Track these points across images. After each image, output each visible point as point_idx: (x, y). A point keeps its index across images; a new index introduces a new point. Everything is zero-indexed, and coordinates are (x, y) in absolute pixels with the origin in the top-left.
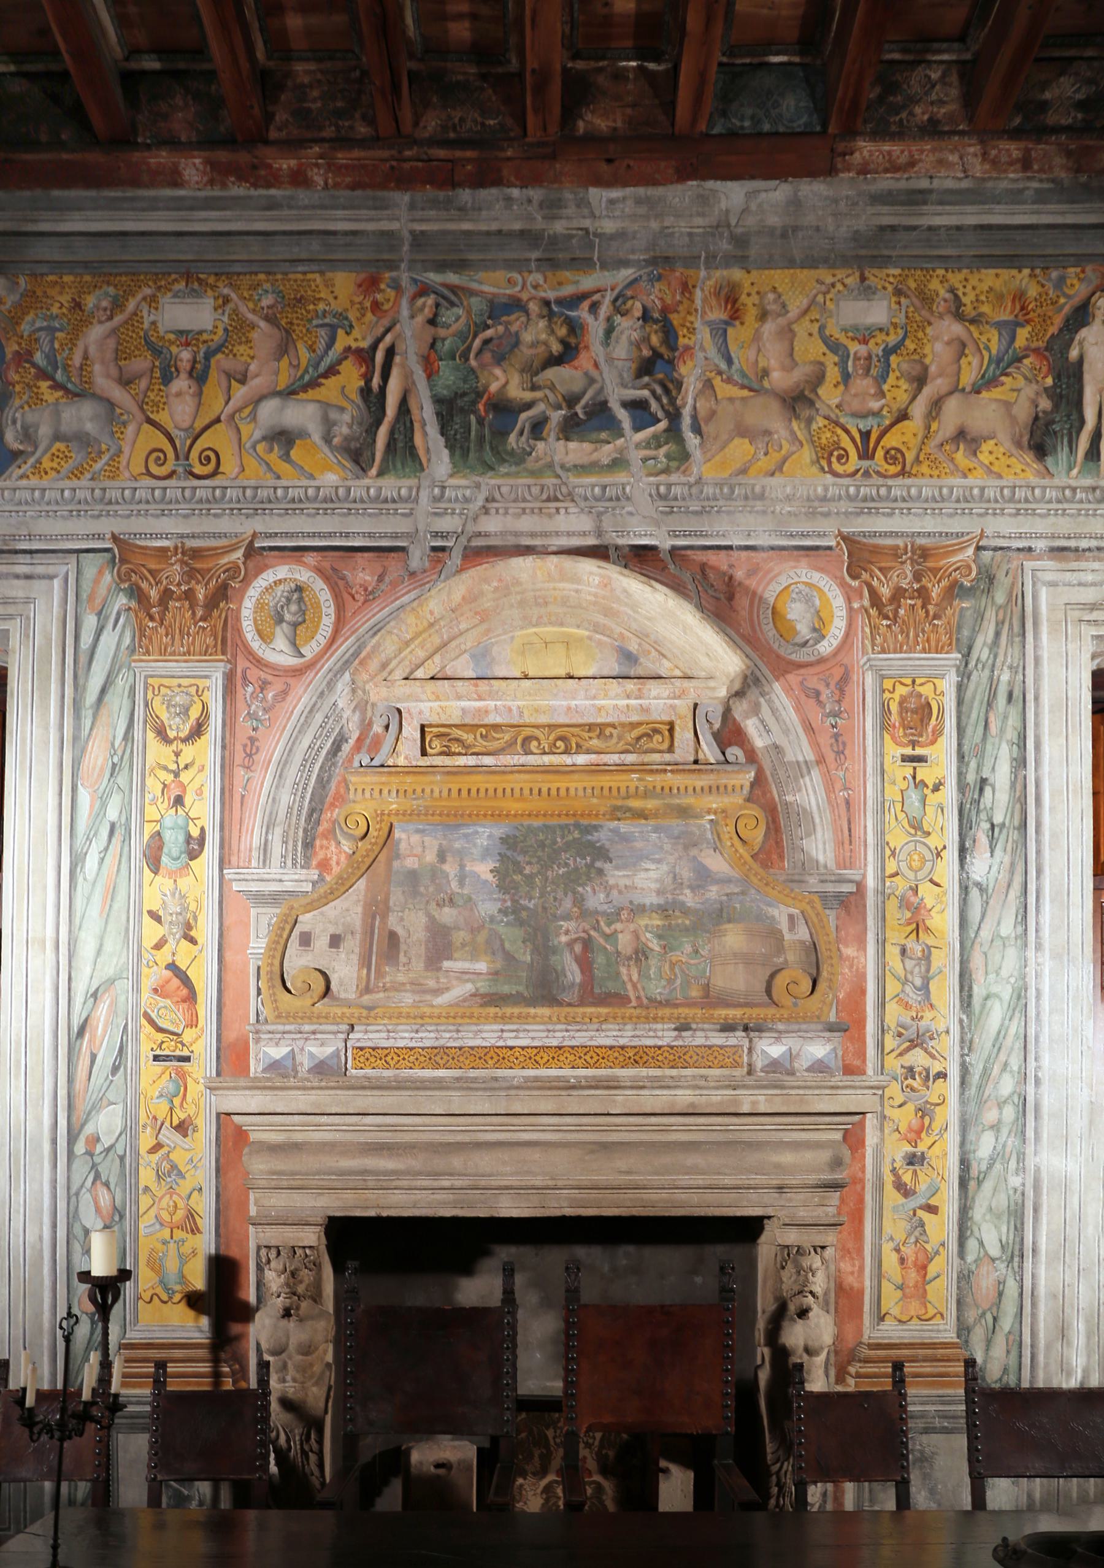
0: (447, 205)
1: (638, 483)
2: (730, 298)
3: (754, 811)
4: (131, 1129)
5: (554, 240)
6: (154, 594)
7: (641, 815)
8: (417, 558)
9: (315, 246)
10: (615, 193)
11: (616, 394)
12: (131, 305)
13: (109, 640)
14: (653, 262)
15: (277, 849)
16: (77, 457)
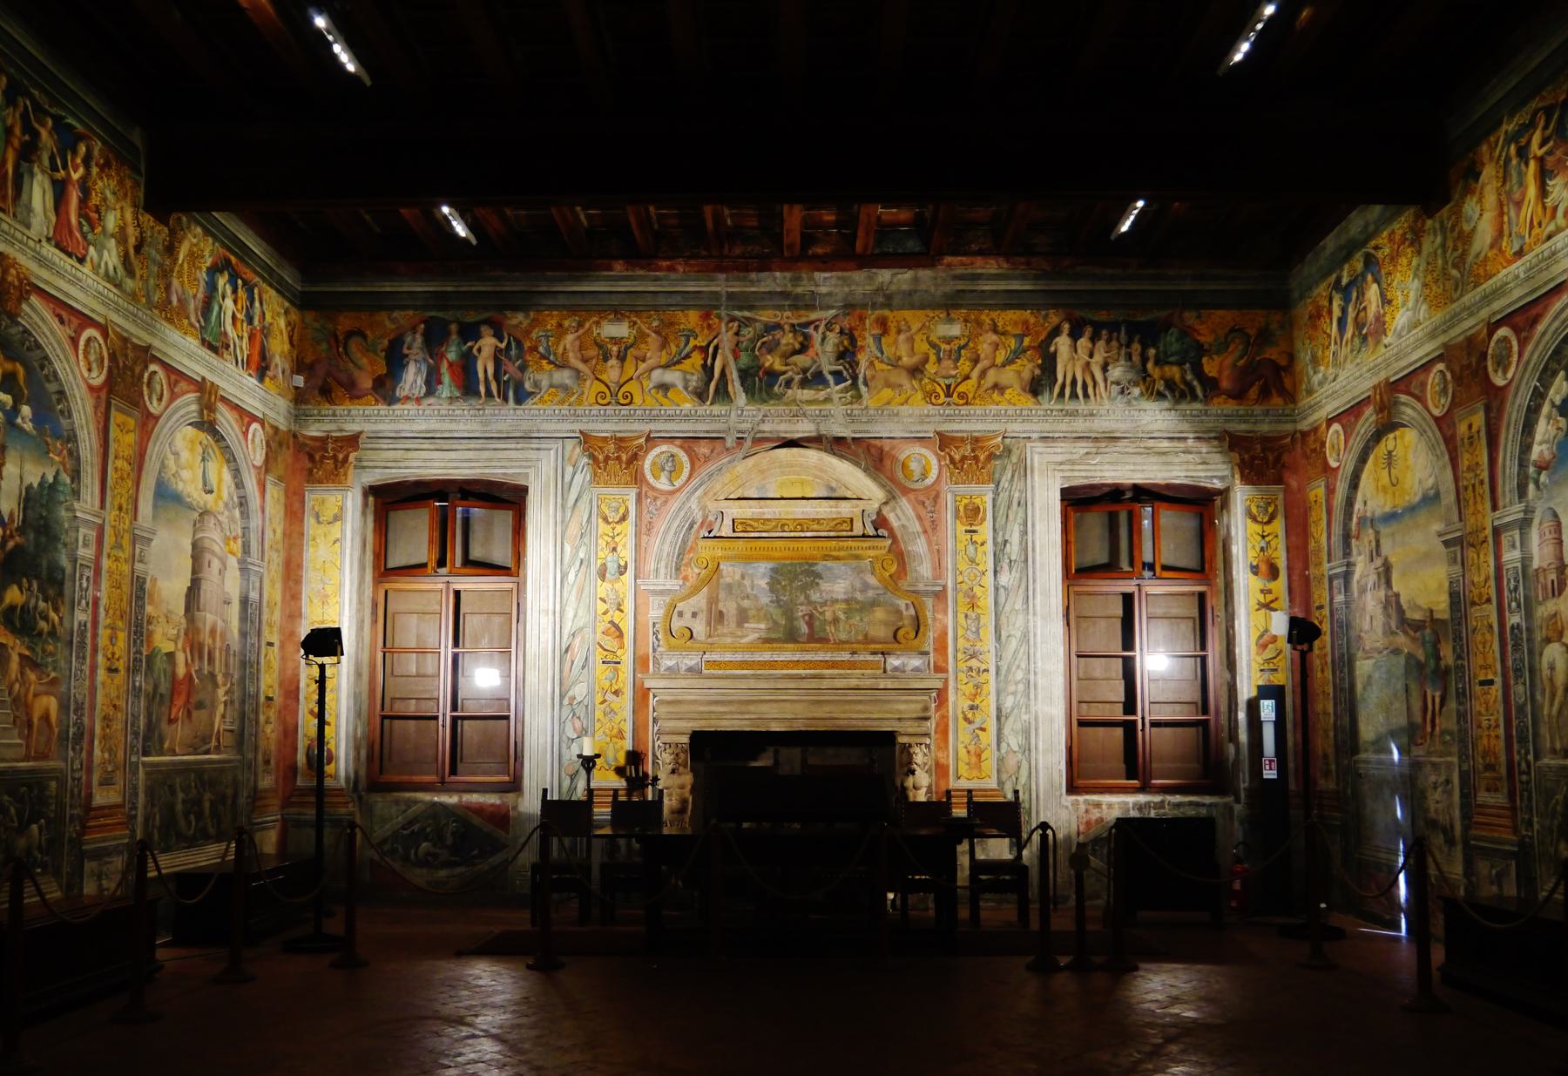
0: (744, 279)
1: (837, 409)
2: (883, 323)
3: (891, 556)
4: (591, 693)
5: (797, 297)
7: (837, 558)
8: (730, 442)
9: (679, 298)
10: (827, 275)
11: (827, 368)
12: (587, 325)
13: (579, 478)
14: (845, 306)
15: (662, 571)
16: (561, 395)
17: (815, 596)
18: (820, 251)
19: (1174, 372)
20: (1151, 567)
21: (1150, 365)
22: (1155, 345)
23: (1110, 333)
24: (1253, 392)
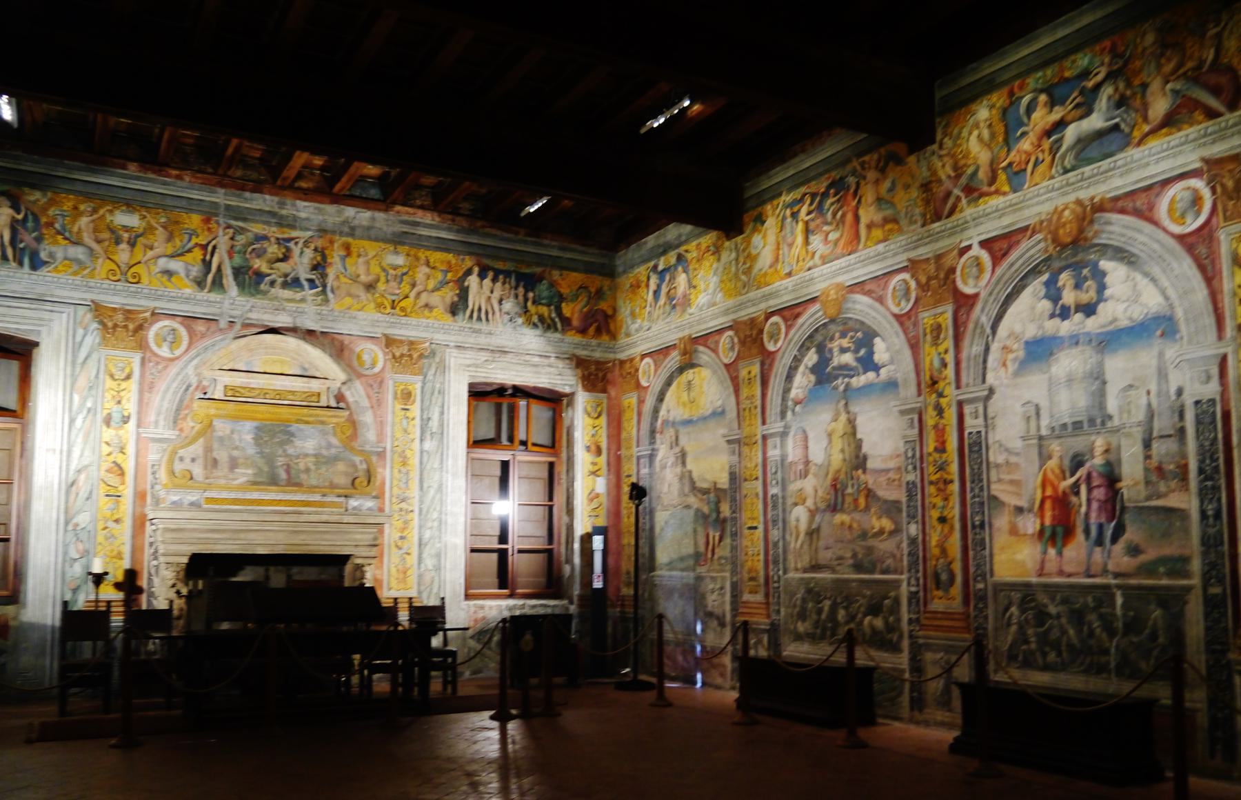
0: (239, 196)
2: (347, 248)
4: (94, 520)
5: (282, 217)
6: (110, 324)
7: (307, 423)
9: (184, 203)
10: (306, 204)
11: (304, 274)
12: (101, 212)
13: (89, 340)
14: (319, 231)
15: (162, 423)
16: (75, 267)
17: (291, 451)
18: (304, 185)
19: (544, 310)
20: (524, 443)
21: (529, 304)
22: (532, 290)
23: (505, 277)
24: (592, 330)
